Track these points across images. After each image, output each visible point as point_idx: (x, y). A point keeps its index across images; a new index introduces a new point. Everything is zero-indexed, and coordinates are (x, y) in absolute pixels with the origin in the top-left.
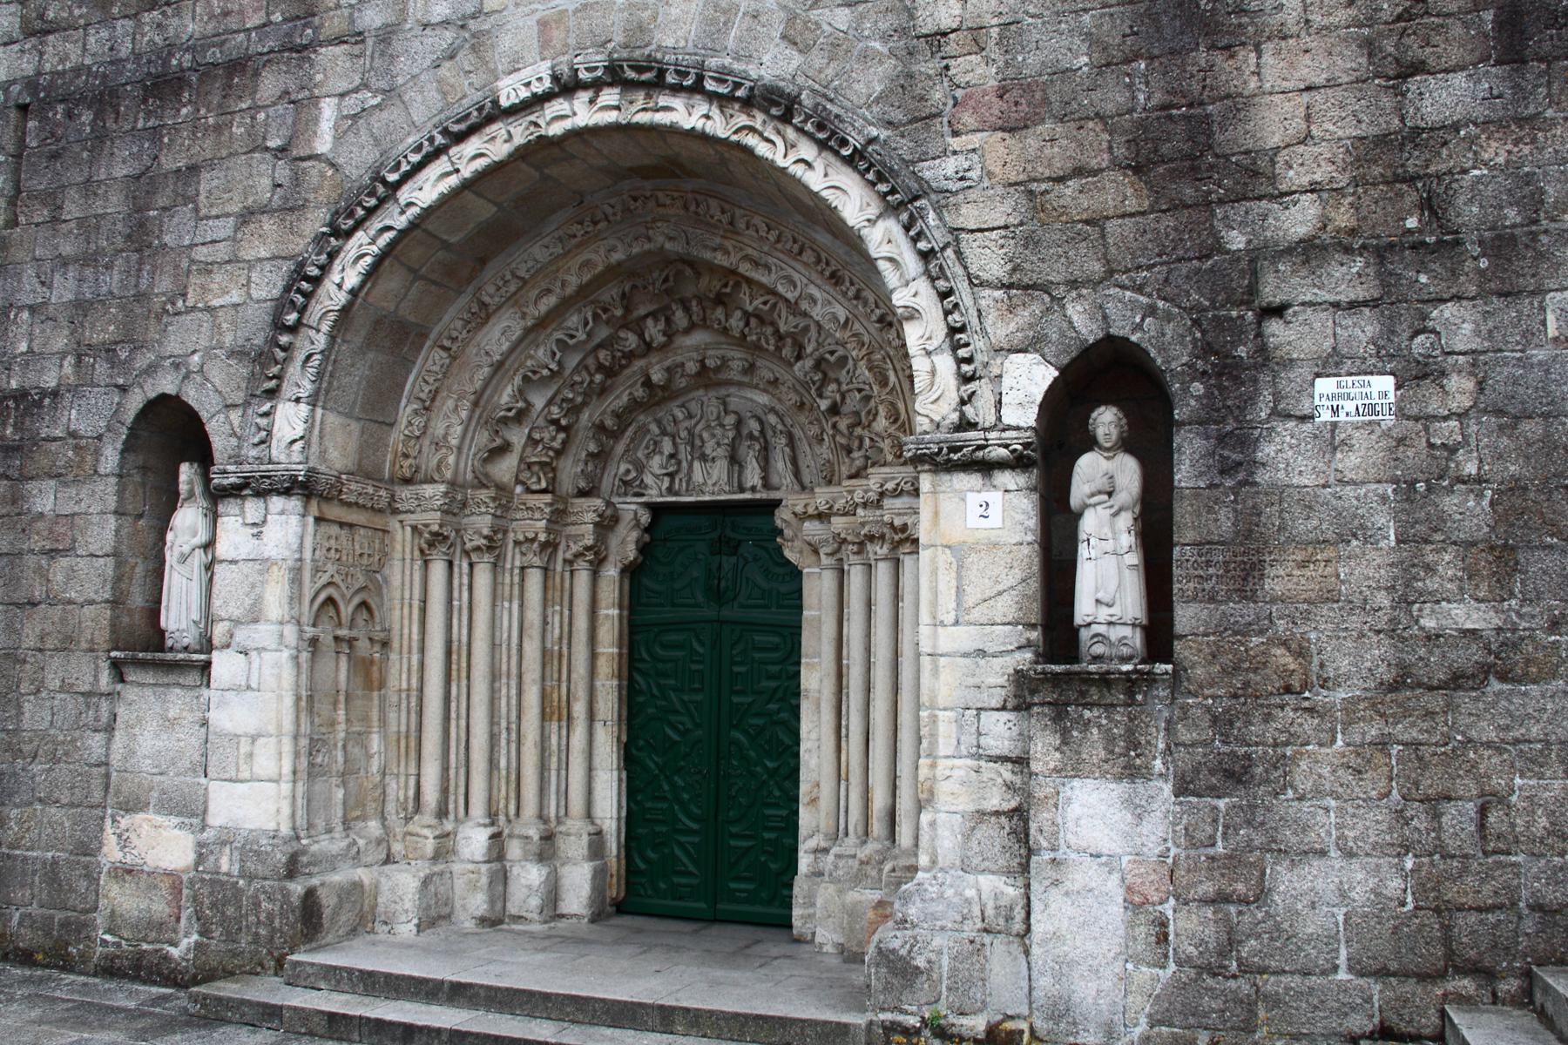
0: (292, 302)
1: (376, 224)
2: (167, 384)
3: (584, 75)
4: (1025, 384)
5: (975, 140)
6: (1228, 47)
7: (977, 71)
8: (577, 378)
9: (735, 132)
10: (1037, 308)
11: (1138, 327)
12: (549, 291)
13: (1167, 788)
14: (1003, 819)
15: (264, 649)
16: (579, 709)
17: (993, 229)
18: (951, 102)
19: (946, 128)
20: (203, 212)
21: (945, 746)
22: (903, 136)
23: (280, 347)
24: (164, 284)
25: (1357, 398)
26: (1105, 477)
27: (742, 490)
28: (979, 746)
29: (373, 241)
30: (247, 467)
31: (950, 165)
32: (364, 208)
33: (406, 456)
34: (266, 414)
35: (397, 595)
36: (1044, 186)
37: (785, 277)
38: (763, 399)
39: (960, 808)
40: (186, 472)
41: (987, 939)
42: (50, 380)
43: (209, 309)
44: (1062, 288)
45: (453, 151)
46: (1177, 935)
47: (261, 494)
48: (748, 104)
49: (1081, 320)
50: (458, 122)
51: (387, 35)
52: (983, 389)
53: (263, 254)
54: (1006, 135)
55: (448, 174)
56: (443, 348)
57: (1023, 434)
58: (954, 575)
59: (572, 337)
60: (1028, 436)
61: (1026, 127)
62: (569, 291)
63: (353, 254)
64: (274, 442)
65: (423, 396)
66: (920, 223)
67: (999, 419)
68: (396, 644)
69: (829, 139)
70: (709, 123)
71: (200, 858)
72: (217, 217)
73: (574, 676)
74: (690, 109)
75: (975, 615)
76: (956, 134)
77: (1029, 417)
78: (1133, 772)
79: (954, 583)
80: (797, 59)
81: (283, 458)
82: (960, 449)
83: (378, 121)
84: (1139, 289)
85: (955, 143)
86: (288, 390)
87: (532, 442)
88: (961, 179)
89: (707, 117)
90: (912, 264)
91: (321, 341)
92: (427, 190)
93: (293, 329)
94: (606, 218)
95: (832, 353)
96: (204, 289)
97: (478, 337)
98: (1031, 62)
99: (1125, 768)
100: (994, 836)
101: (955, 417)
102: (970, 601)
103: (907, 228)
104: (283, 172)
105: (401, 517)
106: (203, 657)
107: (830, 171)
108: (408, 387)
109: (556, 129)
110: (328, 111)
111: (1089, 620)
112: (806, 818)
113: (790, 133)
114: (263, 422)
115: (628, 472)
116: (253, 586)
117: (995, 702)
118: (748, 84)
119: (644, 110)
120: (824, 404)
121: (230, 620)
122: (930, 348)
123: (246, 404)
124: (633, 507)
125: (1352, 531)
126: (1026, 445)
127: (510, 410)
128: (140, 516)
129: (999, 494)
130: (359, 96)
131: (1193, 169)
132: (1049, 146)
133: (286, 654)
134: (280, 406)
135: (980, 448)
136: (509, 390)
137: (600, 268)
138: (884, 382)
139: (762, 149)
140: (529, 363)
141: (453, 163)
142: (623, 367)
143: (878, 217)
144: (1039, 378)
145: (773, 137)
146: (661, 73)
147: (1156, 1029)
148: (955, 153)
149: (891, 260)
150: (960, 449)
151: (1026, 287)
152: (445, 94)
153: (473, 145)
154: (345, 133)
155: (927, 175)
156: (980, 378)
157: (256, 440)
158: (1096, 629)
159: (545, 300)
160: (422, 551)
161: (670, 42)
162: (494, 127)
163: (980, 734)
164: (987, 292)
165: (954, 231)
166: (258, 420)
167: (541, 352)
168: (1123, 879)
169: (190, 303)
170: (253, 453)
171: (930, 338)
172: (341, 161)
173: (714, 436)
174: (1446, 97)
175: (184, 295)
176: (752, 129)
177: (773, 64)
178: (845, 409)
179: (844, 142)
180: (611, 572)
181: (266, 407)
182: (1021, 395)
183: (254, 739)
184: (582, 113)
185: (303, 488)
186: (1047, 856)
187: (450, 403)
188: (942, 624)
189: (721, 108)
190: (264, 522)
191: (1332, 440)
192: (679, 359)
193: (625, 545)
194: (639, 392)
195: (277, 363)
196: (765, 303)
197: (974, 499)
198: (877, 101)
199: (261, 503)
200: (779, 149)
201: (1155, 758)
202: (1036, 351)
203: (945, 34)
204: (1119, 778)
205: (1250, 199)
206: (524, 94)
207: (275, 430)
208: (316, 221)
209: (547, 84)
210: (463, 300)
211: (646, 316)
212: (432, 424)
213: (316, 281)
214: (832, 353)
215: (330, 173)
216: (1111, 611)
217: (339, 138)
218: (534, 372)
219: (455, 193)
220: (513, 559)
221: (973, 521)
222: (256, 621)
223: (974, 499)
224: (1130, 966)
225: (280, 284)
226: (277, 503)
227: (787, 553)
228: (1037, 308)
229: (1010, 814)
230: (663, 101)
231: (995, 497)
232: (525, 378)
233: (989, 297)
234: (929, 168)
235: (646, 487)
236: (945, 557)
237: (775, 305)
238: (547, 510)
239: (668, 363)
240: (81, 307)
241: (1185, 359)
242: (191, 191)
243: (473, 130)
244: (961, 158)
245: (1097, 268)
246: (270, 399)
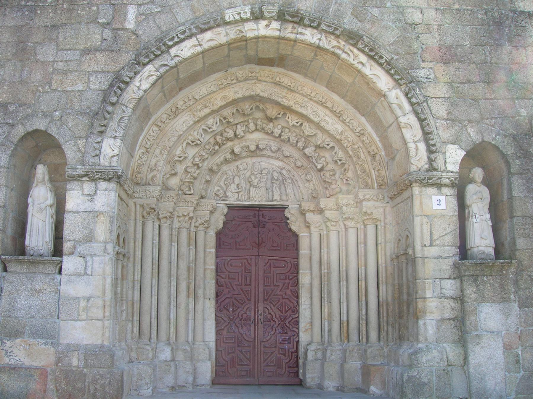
0: (115, 92)
1: (158, 62)
2: (40, 124)
3: (266, 14)
4: (453, 157)
5: (431, 65)
6: (516, 46)
7: (431, 40)
8: (207, 147)
9: (332, 48)
10: (457, 128)
11: (494, 139)
12: (206, 107)
13: (516, 305)
14: (451, 321)
15: (95, 255)
16: (200, 292)
17: (440, 98)
18: (421, 50)
19: (419, 59)
20: (61, 47)
21: (429, 294)
22: (403, 59)
23: (107, 112)
24: (37, 76)
27: (273, 201)
28: (441, 293)
29: (157, 71)
30: (87, 167)
31: (422, 73)
32: (154, 54)
33: (139, 173)
34: (99, 142)
35: (132, 236)
36: (457, 85)
37: (313, 112)
38: (280, 164)
39: (435, 318)
40: (41, 170)
41: (449, 368)
43: (63, 91)
44: (466, 122)
45: (198, 36)
46: (523, 359)
47: (94, 180)
48: (338, 37)
49: (473, 134)
50: (204, 24)
52: (440, 156)
53: (96, 69)
54: (442, 65)
55: (196, 46)
56: (157, 125)
57: (454, 174)
58: (429, 227)
59: (209, 128)
60: (456, 175)
61: (449, 63)
62: (216, 108)
63: (146, 74)
64: (102, 157)
65: (147, 146)
66: (413, 92)
67: (446, 168)
68: (131, 259)
69: (374, 56)
70: (321, 42)
71: (59, 360)
72: (70, 50)
73: (198, 278)
74: (312, 35)
75: (437, 242)
76: (423, 61)
77: (456, 168)
78: (505, 300)
79: (429, 230)
80: (359, 24)
81: (106, 164)
82: (432, 178)
83: (160, 19)
84: (493, 126)
85: (424, 65)
86: (110, 132)
87: (186, 171)
88: (426, 78)
89: (320, 40)
90: (407, 106)
91: (129, 111)
92: (186, 49)
93: (113, 104)
94: (237, 79)
95: (328, 145)
96: (62, 82)
97: (172, 123)
98: (448, 41)
99: (501, 298)
100: (449, 329)
101: (427, 166)
102: (435, 237)
103: (406, 95)
104: (107, 33)
105: (134, 200)
106: (59, 258)
107: (372, 68)
108: (140, 141)
109: (250, 35)
110: (132, 12)
111: (478, 245)
112: (304, 338)
113: (355, 51)
114: (97, 146)
115: (218, 190)
116: (88, 224)
117: (447, 276)
118: (341, 30)
119: (291, 32)
120: (319, 166)
121: (74, 240)
122: (416, 140)
123: (87, 138)
124: (221, 205)
126: (456, 179)
127: (180, 157)
128: (12, 190)
129: (444, 197)
130: (149, 6)
131: (507, 86)
133: (107, 258)
134: (105, 140)
135: (439, 178)
136: (180, 148)
137: (230, 100)
138: (359, 158)
139: (344, 56)
140: (190, 137)
141: (199, 42)
142: (223, 144)
143: (393, 88)
144: (459, 154)
145: (348, 52)
146: (302, 19)
147: (518, 396)
148: (424, 68)
149: (398, 105)
150: (432, 178)
151: (453, 120)
152: (194, 12)
153: (208, 35)
154: (142, 21)
155: (414, 74)
156: (438, 152)
157: (94, 154)
158: (480, 248)
159: (204, 110)
160: (143, 217)
161: (304, 8)
162: (219, 29)
163: (441, 289)
164: (439, 121)
165: (425, 96)
166: (95, 145)
167: (196, 133)
168: (503, 340)
169: (53, 88)
170: (91, 160)
171: (415, 136)
172: (139, 33)
173: (256, 178)
175: (50, 84)
176: (339, 48)
177: (349, 22)
178: (326, 168)
179: (381, 57)
180: (212, 233)
181: (99, 139)
182: (453, 160)
183: (88, 300)
185: (116, 178)
186: (474, 333)
187: (158, 151)
188: (425, 246)
189: (326, 37)
190: (95, 194)
192: (247, 144)
193: (218, 221)
194: (229, 156)
195: (105, 119)
196: (297, 123)
197: (435, 198)
198: (392, 44)
199: (93, 185)
201: (511, 294)
202: (458, 144)
203: (416, 25)
204: (499, 303)
205: (527, 99)
206: (237, 17)
207: (102, 151)
208: (126, 58)
209: (249, 15)
210: (168, 106)
211: (237, 124)
212: (149, 159)
213: (127, 83)
214: (328, 145)
215: (133, 37)
216: (487, 241)
217: (138, 24)
218: (193, 142)
219: (198, 54)
220: (176, 225)
221: (435, 207)
222: (90, 241)
223: (435, 198)
224: (507, 373)
225: (107, 84)
226: (103, 185)
227: (294, 228)
228: (457, 128)
229: (454, 319)
230: (300, 30)
231: (442, 198)
232: (188, 143)
233: (439, 123)
234: (414, 72)
235: (226, 197)
236: (425, 220)
237: (301, 124)
238: (195, 202)
239: (242, 145)
241: (512, 151)
242: (54, 36)
243: (210, 28)
244: (426, 70)
245: (476, 115)
246: (100, 136)
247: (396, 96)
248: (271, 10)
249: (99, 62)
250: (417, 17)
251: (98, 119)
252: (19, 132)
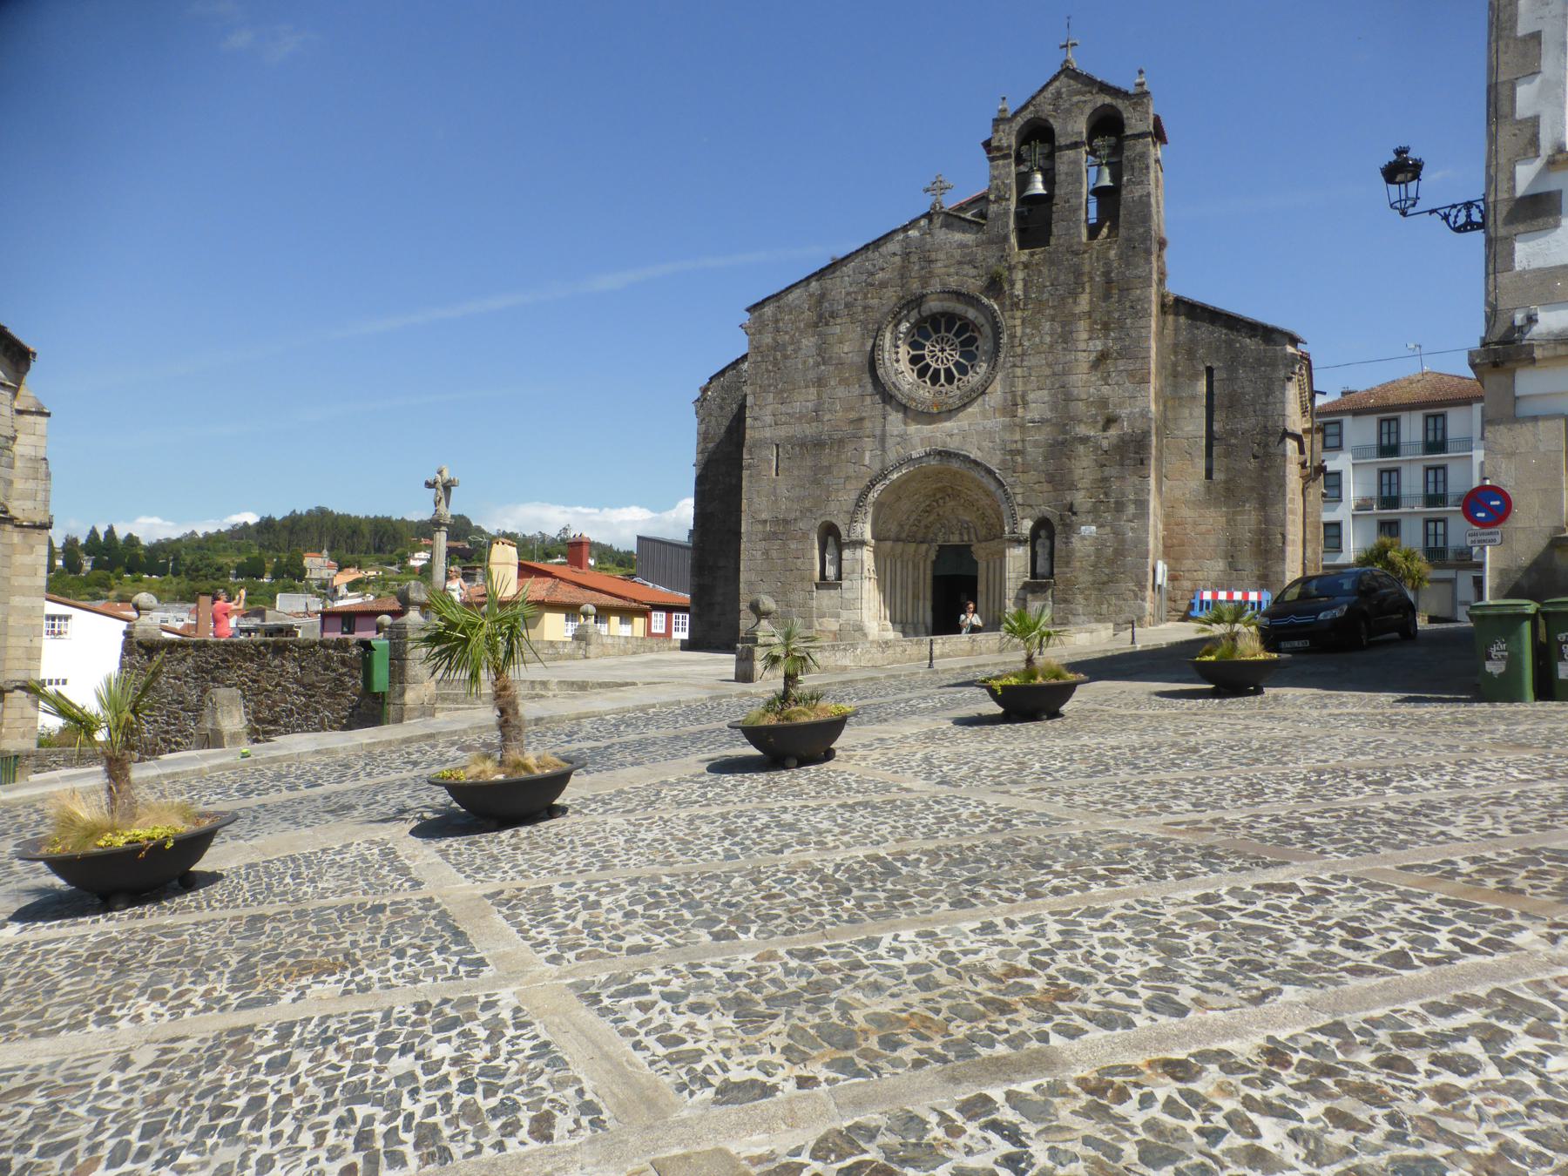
25: (1089, 530)
42: (793, 516)
49: (1037, 513)
110: (867, 454)
180: (929, 563)
191: (1083, 538)
252: (819, 522)
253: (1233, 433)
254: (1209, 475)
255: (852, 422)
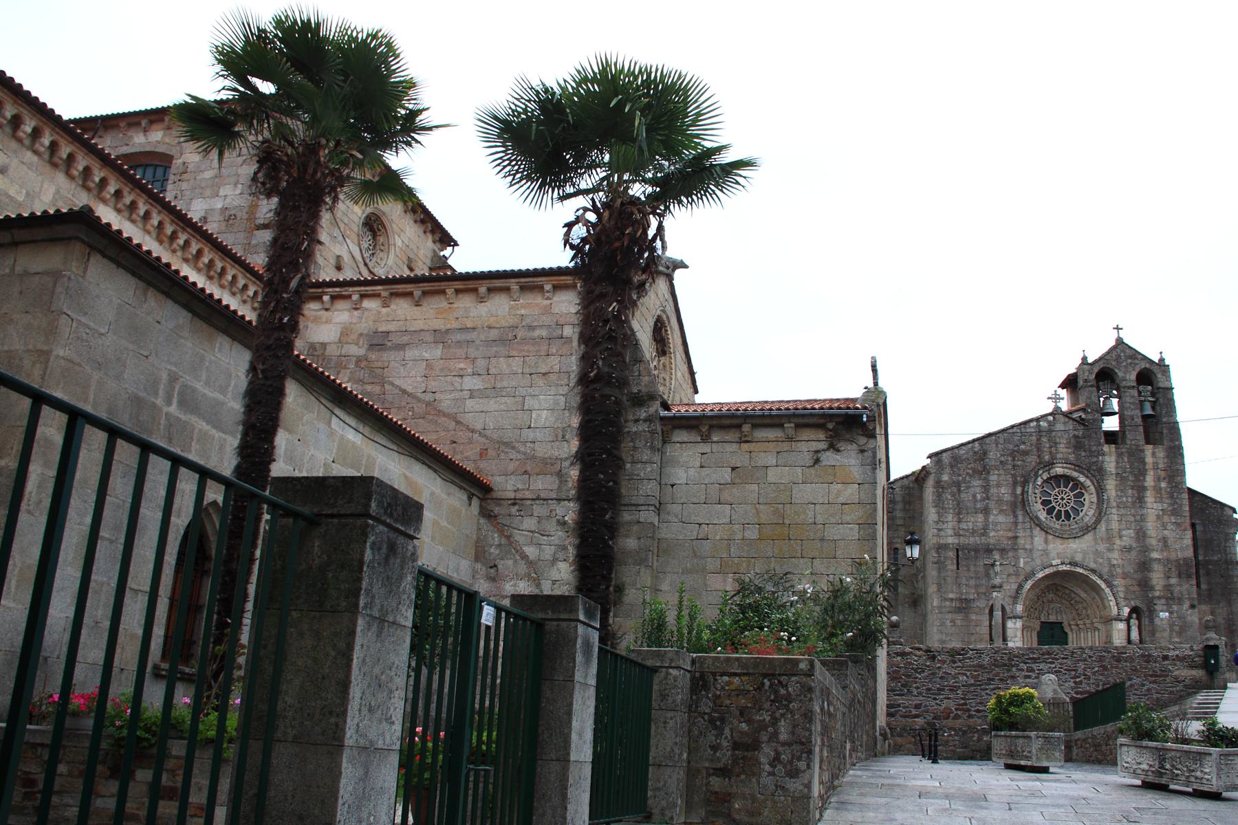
25: (1164, 615)
26: (1134, 622)
51: (1031, 550)
69: (1101, 577)
92: (1040, 575)
125: (1164, 630)
132: (1129, 581)
174: (1173, 581)
177: (1092, 565)
184: (1064, 568)
200: (1094, 578)
208: (1022, 577)
240: (977, 586)
247: (1107, 590)
248: (1067, 561)
249: (1013, 579)
250: (1115, 562)
251: (1015, 598)
253: (1208, 562)
254: (1198, 585)
255: (1009, 538)
